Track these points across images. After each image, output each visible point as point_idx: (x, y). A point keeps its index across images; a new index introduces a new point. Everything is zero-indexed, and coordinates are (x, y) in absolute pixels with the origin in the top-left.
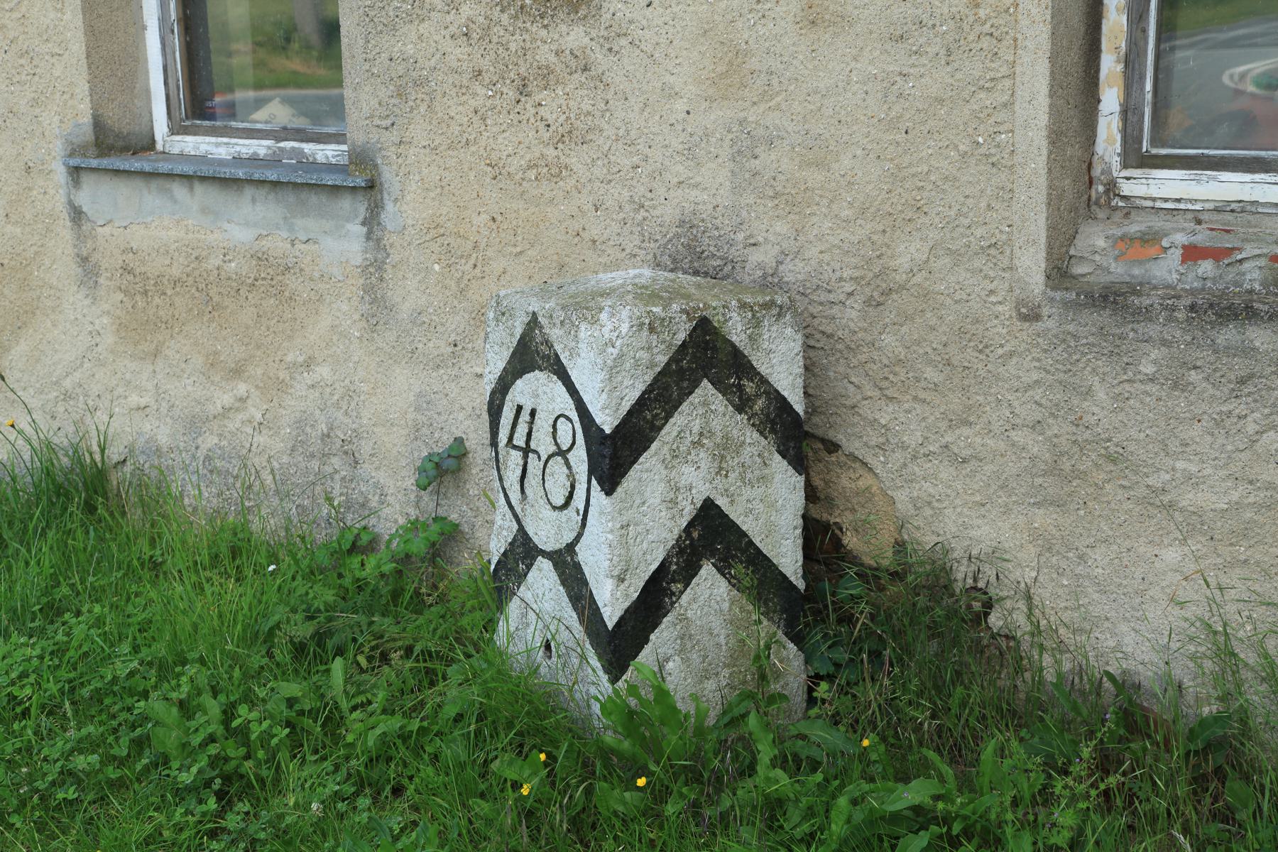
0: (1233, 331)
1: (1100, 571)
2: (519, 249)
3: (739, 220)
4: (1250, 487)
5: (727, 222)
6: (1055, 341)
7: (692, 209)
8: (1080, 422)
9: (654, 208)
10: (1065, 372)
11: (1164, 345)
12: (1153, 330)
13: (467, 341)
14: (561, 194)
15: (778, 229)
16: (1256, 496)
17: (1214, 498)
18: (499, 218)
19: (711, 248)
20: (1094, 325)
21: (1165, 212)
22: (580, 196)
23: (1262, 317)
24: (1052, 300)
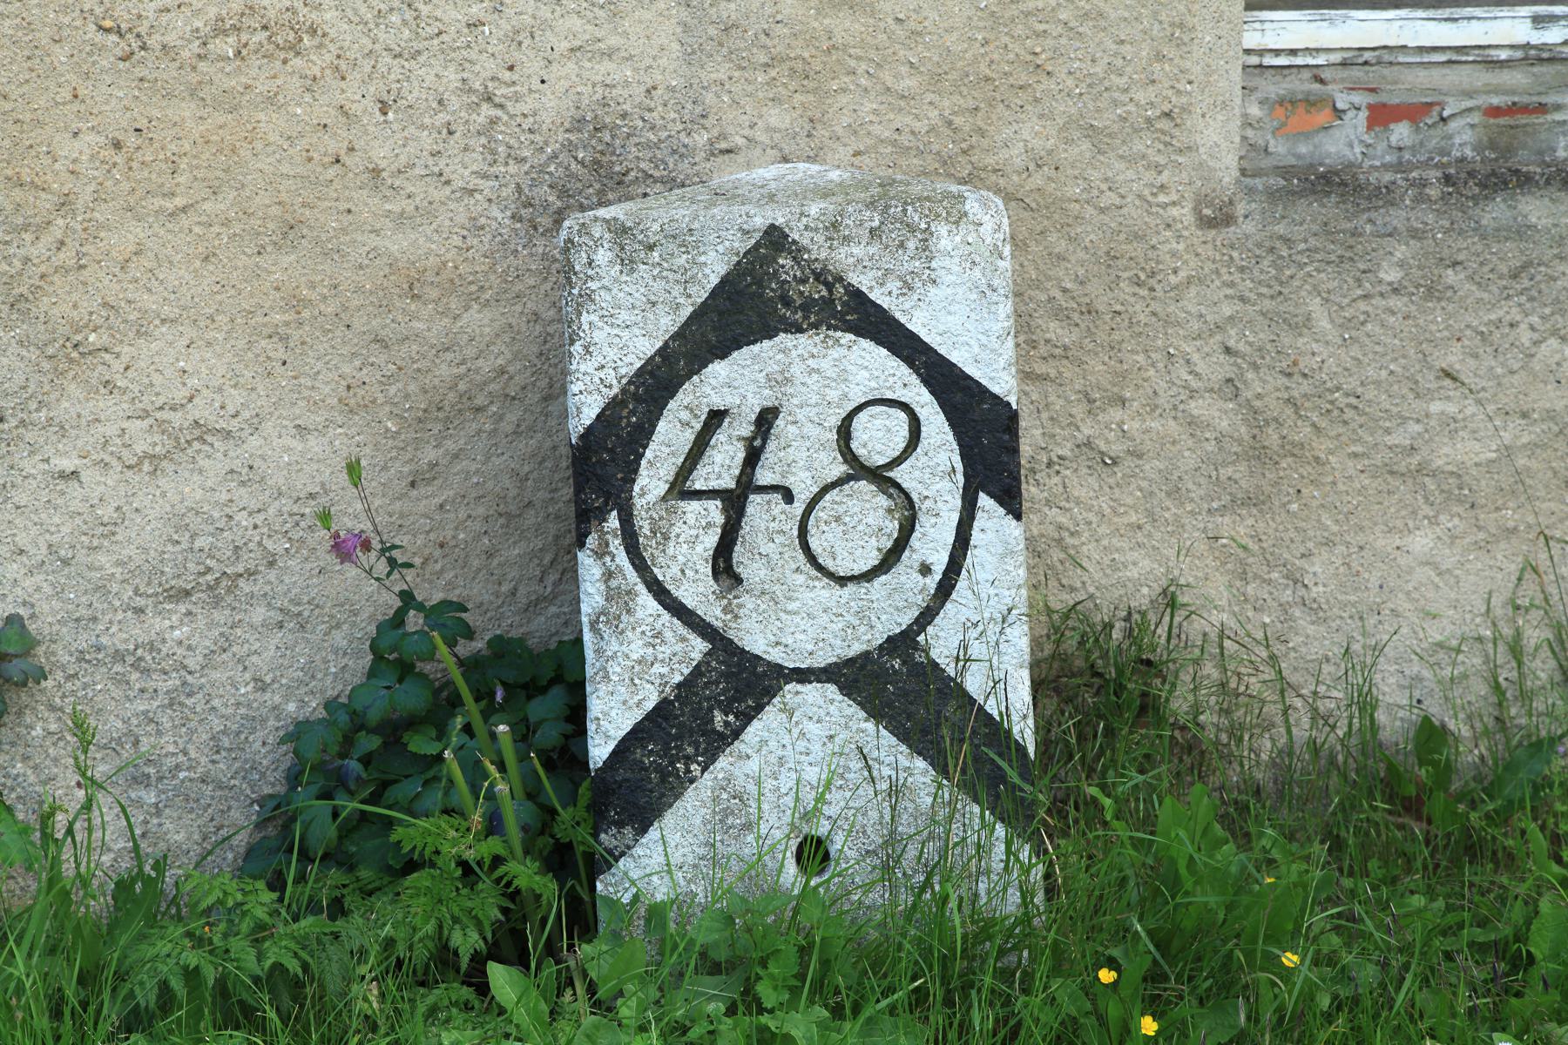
0: (1502, 205)
1: (1321, 589)
2: (179, 201)
3: (699, 110)
4: (1523, 422)
5: (673, 115)
6: (1258, 252)
7: (598, 96)
8: (1296, 370)
9: (517, 98)
10: (1272, 297)
11: (1413, 237)
12: (1397, 218)
13: (33, 405)
14: (296, 82)
15: (774, 121)
16: (1530, 433)
17: (1477, 446)
18: (132, 140)
19: (642, 165)
20: (1314, 221)
21: (1273, 71)
22: (343, 84)
23: (1537, 182)
24: (1251, 191)
